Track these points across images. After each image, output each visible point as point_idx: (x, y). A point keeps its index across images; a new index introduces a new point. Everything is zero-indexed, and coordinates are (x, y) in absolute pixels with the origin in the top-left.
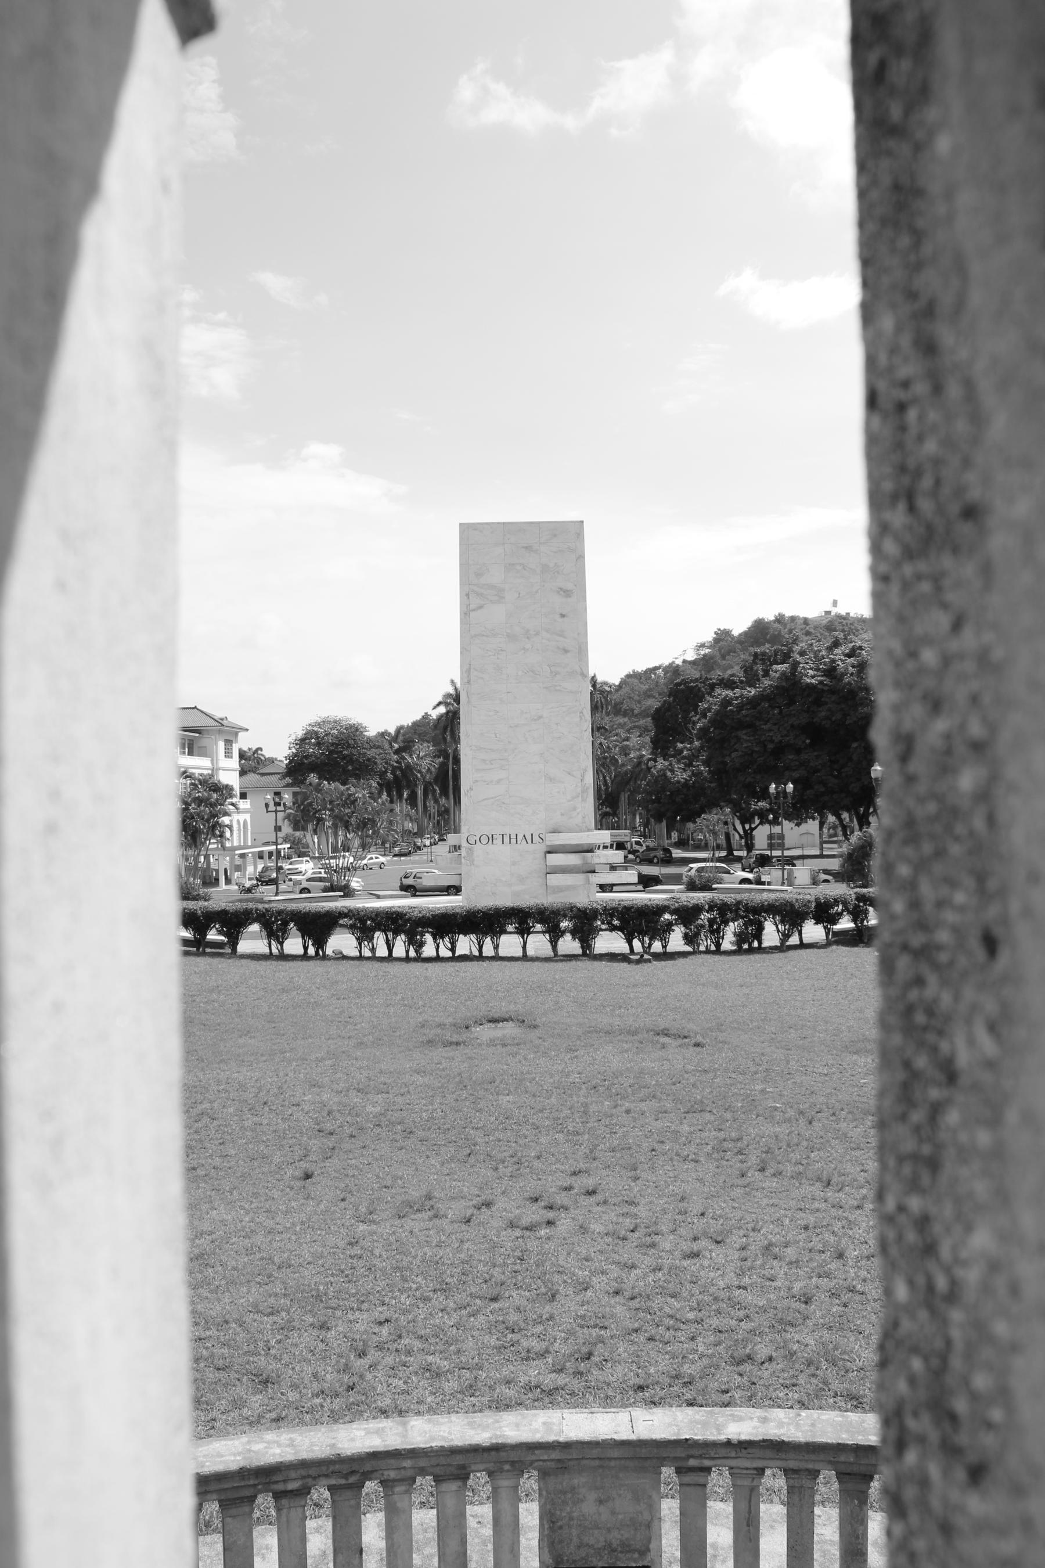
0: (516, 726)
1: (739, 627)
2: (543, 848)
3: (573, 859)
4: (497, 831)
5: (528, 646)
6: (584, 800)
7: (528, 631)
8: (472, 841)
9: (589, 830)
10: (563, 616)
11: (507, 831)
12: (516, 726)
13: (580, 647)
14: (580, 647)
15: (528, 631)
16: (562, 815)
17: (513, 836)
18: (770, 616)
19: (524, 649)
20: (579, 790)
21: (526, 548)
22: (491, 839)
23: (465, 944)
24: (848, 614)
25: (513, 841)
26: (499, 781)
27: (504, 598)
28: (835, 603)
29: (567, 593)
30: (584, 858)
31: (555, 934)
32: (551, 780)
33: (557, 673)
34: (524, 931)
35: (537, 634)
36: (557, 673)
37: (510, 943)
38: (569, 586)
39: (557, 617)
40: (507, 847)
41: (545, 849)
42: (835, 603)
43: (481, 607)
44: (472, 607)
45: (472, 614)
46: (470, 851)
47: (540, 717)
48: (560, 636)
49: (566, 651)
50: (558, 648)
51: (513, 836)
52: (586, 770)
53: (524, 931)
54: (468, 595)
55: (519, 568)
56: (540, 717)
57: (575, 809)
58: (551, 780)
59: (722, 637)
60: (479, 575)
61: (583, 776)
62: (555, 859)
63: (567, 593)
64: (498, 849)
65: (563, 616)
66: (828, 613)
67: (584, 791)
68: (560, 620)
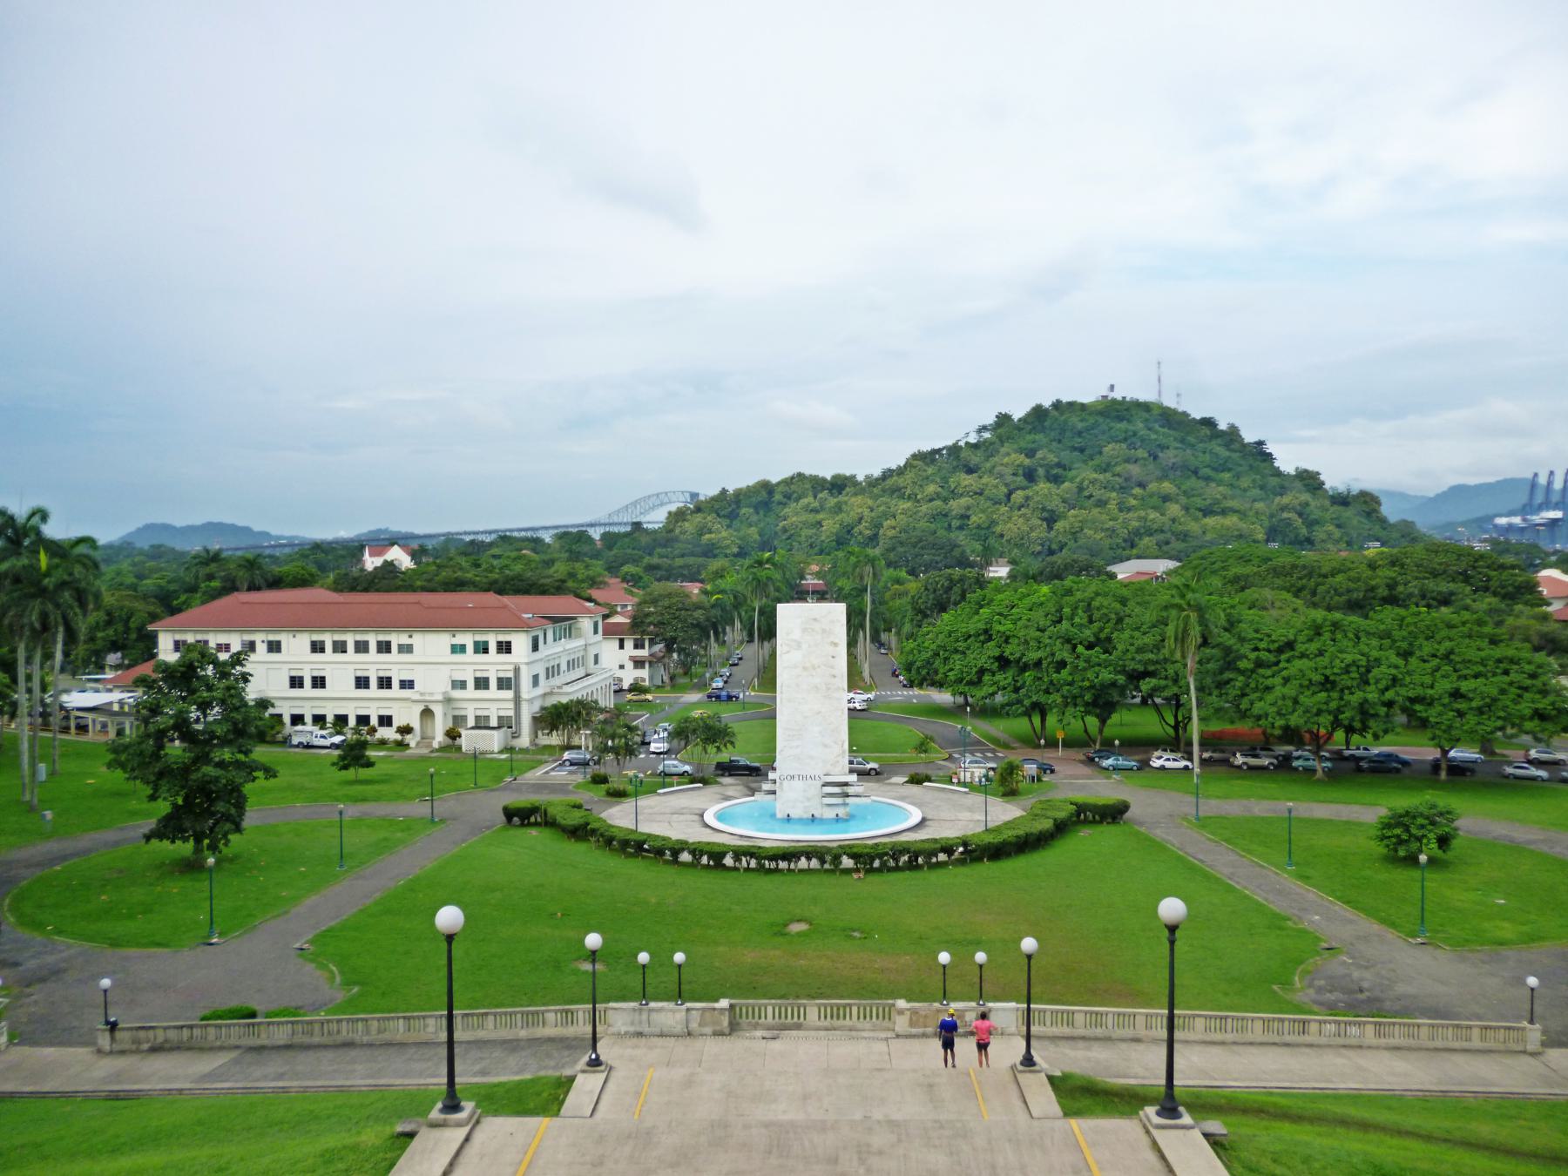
3: (837, 790)
23: (783, 865)
32: (826, 746)
37: (803, 863)
53: (809, 859)
58: (826, 746)
64: (797, 784)
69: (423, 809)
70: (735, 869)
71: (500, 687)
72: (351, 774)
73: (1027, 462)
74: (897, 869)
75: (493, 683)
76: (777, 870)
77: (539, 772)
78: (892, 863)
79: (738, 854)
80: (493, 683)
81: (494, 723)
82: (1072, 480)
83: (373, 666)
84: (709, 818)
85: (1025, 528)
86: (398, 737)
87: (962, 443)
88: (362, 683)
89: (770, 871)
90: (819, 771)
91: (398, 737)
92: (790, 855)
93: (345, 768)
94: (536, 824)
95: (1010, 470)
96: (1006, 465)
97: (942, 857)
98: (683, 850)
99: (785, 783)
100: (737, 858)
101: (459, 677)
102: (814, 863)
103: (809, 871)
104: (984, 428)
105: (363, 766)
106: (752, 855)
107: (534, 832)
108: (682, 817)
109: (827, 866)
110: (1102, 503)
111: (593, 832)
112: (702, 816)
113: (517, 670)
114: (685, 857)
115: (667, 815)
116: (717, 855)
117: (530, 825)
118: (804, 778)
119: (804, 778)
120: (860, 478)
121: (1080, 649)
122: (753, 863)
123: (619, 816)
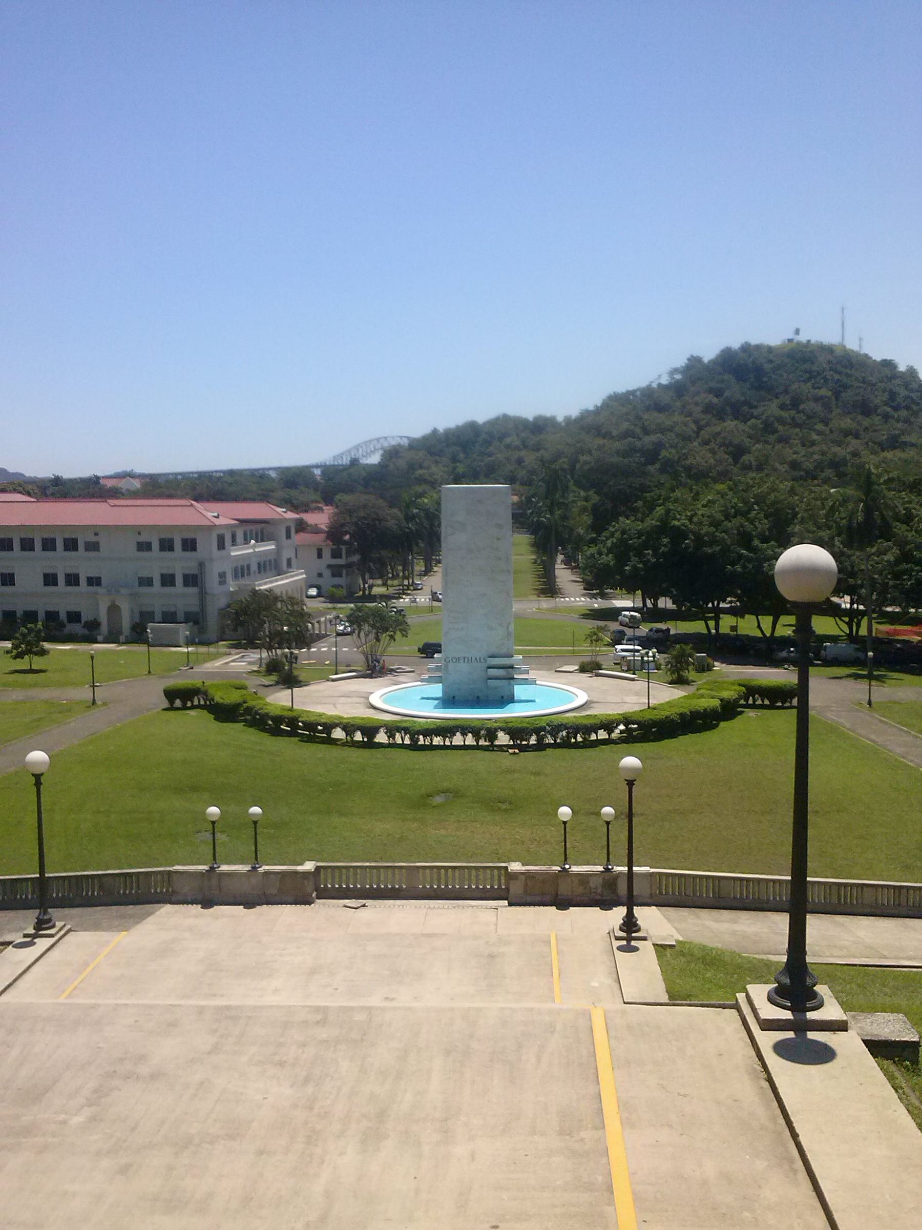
1: (709, 353)
2: (486, 666)
3: (501, 672)
4: (462, 655)
11: (466, 655)
18: (736, 344)
23: (437, 741)
24: (809, 341)
26: (462, 629)
28: (797, 332)
31: (477, 736)
32: (491, 629)
34: (464, 734)
37: (458, 740)
42: (797, 332)
53: (464, 734)
58: (491, 629)
59: (694, 362)
62: (493, 672)
66: (790, 341)
69: (85, 694)
70: (390, 746)
71: (186, 584)
72: (23, 664)
73: (715, 400)
74: (555, 746)
75: (179, 580)
76: (432, 747)
77: (218, 663)
78: (549, 740)
79: (392, 730)
80: (179, 580)
81: (180, 616)
82: (756, 418)
83: (61, 562)
84: (375, 700)
85: (712, 461)
86: (87, 632)
87: (654, 385)
88: (50, 580)
89: (424, 748)
91: (87, 632)
92: (446, 730)
93: (20, 656)
94: (199, 707)
95: (699, 409)
96: (697, 404)
97: (602, 735)
98: (335, 726)
99: (451, 666)
100: (391, 733)
101: (145, 574)
102: (470, 740)
103: (464, 747)
104: (675, 371)
105: (36, 654)
106: (406, 730)
107: (192, 713)
108: (349, 700)
109: (482, 742)
110: (784, 440)
111: (249, 710)
112: (368, 698)
113: (201, 565)
114: (338, 734)
115: (333, 697)
116: (370, 731)
117: (193, 707)
120: (560, 418)
121: (756, 542)
122: (407, 741)
123: (280, 699)
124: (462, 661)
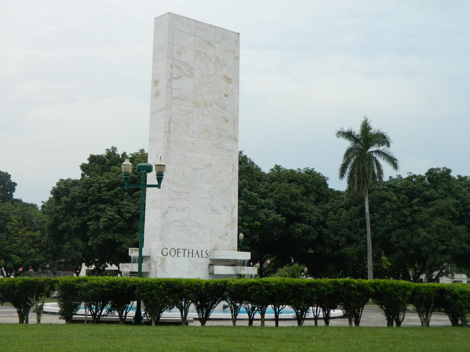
0: (196, 169)
4: (182, 246)
5: (206, 113)
6: (232, 228)
7: (206, 101)
8: (165, 254)
9: (234, 250)
10: (226, 96)
11: (187, 246)
12: (196, 169)
13: (234, 119)
14: (234, 119)
15: (206, 101)
16: (220, 238)
17: (191, 251)
19: (203, 113)
20: (230, 220)
21: (208, 42)
22: (177, 252)
25: (191, 255)
26: (184, 209)
27: (193, 74)
29: (229, 80)
30: (236, 270)
32: (215, 211)
33: (221, 135)
35: (211, 105)
36: (221, 135)
38: (230, 76)
39: (223, 96)
40: (186, 260)
41: (208, 262)
43: (179, 77)
44: (174, 76)
45: (174, 81)
46: (163, 260)
47: (211, 165)
48: (224, 109)
49: (227, 121)
50: (223, 117)
51: (191, 251)
52: (234, 207)
54: (171, 66)
55: (203, 55)
56: (211, 165)
57: (227, 234)
58: (215, 211)
60: (179, 53)
61: (232, 211)
63: (229, 80)
65: (226, 96)
67: (233, 222)
68: (224, 98)
90: (205, 247)
118: (191, 253)
119: (191, 253)
124: (181, 254)
